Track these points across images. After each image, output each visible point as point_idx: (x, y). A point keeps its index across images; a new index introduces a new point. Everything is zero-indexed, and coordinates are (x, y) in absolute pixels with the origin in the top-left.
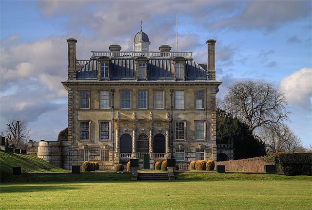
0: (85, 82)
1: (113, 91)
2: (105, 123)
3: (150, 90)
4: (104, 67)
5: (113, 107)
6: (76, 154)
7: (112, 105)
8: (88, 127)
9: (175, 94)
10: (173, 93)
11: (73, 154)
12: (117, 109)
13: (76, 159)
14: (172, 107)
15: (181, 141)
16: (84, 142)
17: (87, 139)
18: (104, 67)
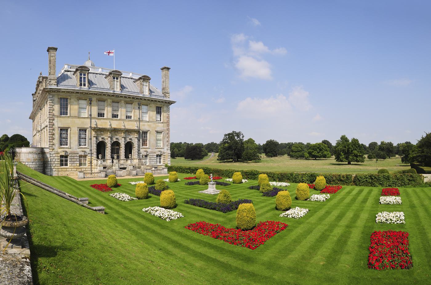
0: (67, 89)
1: (91, 100)
2: (83, 130)
3: (123, 102)
4: (83, 76)
5: (91, 115)
6: (57, 160)
7: (90, 114)
8: (67, 134)
9: (141, 107)
10: (140, 107)
11: (54, 160)
12: (94, 118)
13: (57, 165)
14: (139, 119)
15: (146, 148)
16: (64, 148)
17: (67, 145)
18: (83, 76)
